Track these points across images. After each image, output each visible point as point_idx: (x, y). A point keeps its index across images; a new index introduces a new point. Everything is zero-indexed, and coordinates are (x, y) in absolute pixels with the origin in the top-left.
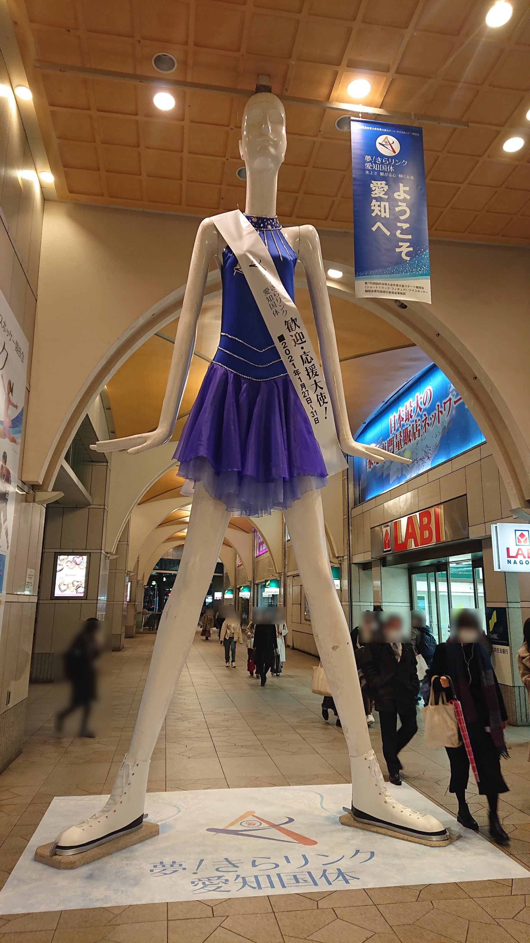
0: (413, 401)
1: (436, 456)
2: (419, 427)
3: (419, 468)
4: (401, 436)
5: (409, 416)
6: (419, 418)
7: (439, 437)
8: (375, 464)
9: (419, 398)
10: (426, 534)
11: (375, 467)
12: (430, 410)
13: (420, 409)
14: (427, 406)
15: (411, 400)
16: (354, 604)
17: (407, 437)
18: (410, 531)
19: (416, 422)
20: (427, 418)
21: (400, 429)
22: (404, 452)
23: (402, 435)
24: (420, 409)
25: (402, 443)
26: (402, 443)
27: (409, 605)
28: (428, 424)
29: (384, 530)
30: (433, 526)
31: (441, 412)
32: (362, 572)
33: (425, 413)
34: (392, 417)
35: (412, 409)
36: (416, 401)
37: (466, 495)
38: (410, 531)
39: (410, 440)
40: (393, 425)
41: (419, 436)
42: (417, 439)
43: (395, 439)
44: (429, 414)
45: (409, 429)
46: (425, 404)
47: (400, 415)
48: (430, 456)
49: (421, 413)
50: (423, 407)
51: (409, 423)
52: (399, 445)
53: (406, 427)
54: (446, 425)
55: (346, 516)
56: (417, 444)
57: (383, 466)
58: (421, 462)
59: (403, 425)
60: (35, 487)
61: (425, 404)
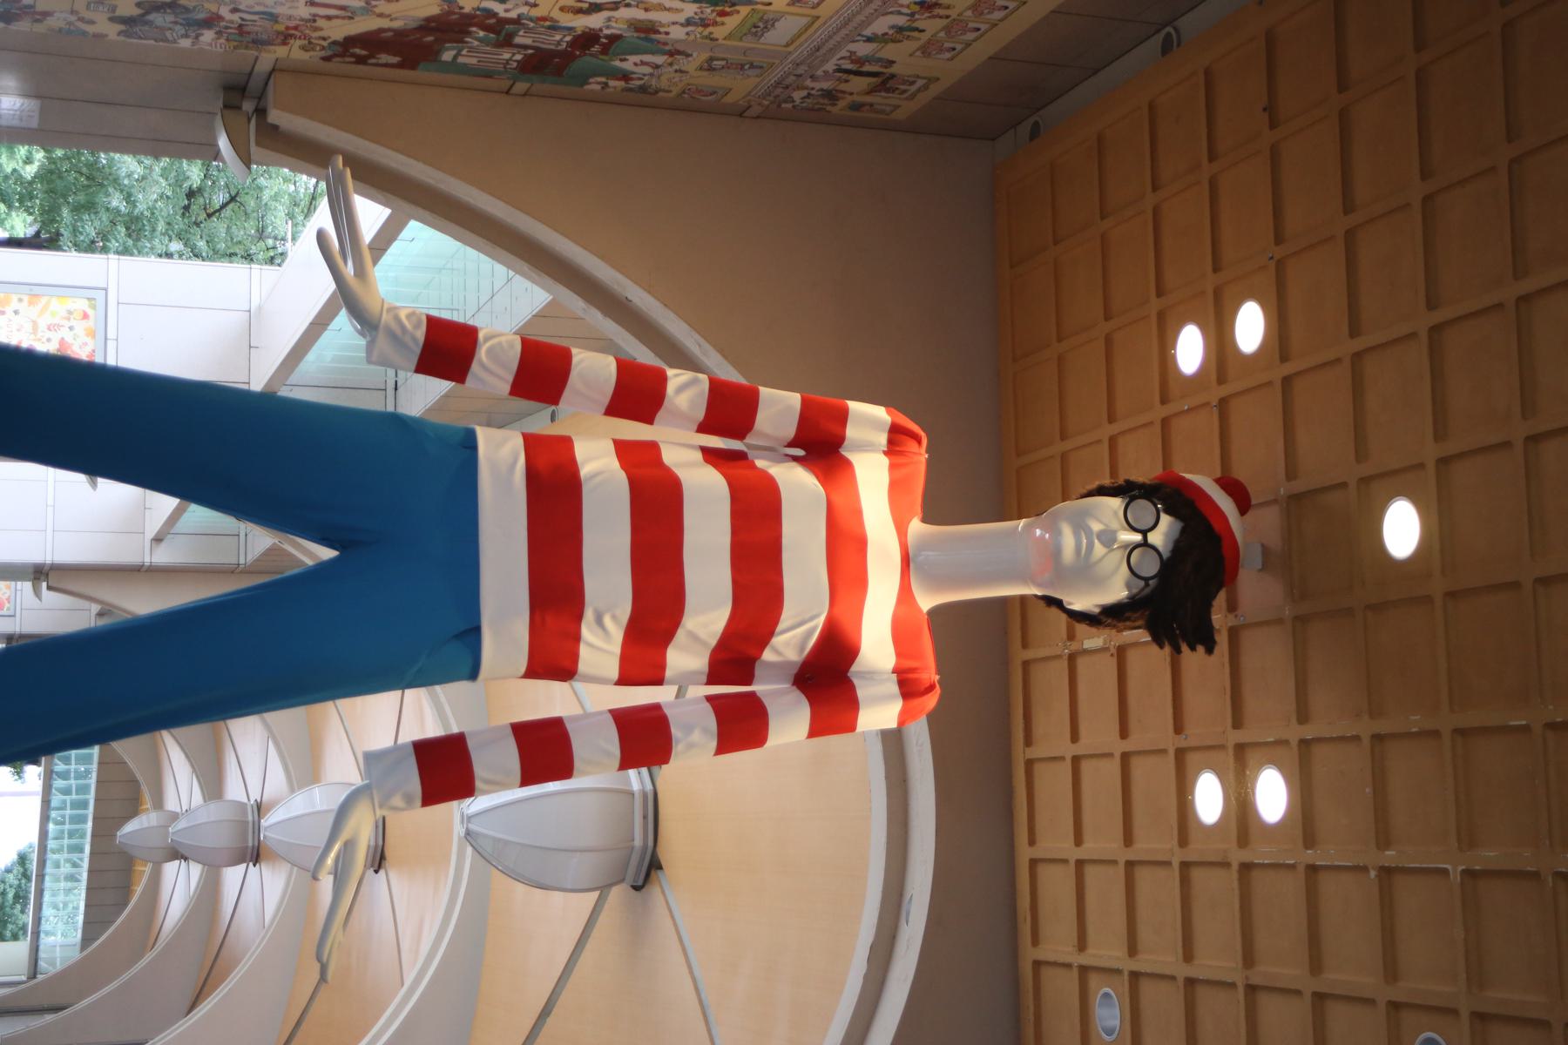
60: (261, 112)
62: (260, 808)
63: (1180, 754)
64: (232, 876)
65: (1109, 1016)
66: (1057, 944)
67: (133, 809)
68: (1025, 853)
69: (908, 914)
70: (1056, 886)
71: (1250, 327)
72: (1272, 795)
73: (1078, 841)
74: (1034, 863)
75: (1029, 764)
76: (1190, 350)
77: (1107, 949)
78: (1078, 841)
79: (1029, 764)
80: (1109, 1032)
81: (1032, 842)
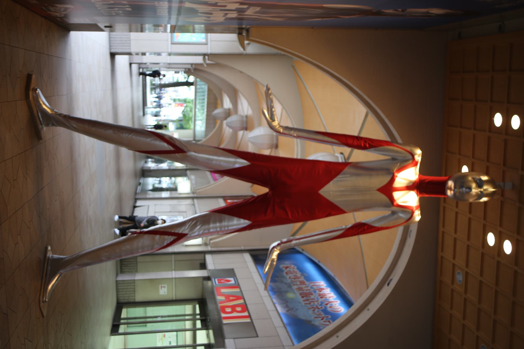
0: (334, 299)
1: (288, 316)
2: (312, 304)
3: (281, 304)
4: (307, 290)
5: (322, 296)
6: (320, 304)
7: (303, 318)
8: (286, 271)
9: (335, 303)
10: (228, 310)
11: (283, 271)
12: (325, 311)
13: (327, 304)
14: (329, 309)
15: (335, 297)
16: (173, 256)
17: (305, 295)
18: (231, 298)
19: (317, 301)
20: (318, 308)
21: (312, 290)
22: (294, 293)
23: (308, 291)
24: (327, 304)
25: (301, 292)
26: (301, 292)
27: (174, 299)
28: (314, 310)
29: (232, 279)
30: (235, 314)
31: (323, 319)
32: (198, 263)
33: (323, 308)
34: (322, 283)
35: (328, 298)
36: (333, 300)
37: (257, 336)
38: (231, 298)
39: (303, 297)
40: (316, 284)
41: (306, 304)
42: (303, 303)
43: (304, 286)
44: (323, 311)
45: (312, 297)
46: (330, 307)
47: (323, 289)
48: (290, 312)
49: (324, 304)
50: (328, 306)
51: (317, 295)
52: (300, 289)
53: (314, 294)
54: (313, 323)
55: (243, 248)
56: (300, 303)
57: (283, 277)
58: (285, 305)
59: (315, 292)
60: (248, 31)
61: (330, 307)
62: (247, 117)
63: (484, 226)
64: (241, 133)
65: (460, 277)
66: (448, 253)
67: (216, 108)
68: (441, 229)
69: (410, 235)
70: (449, 242)
71: (516, 122)
72: (508, 247)
73: (456, 232)
74: (443, 232)
75: (444, 208)
76: (498, 120)
77: (460, 261)
78: (456, 232)
79: (444, 208)
80: (460, 281)
81: (443, 226)
